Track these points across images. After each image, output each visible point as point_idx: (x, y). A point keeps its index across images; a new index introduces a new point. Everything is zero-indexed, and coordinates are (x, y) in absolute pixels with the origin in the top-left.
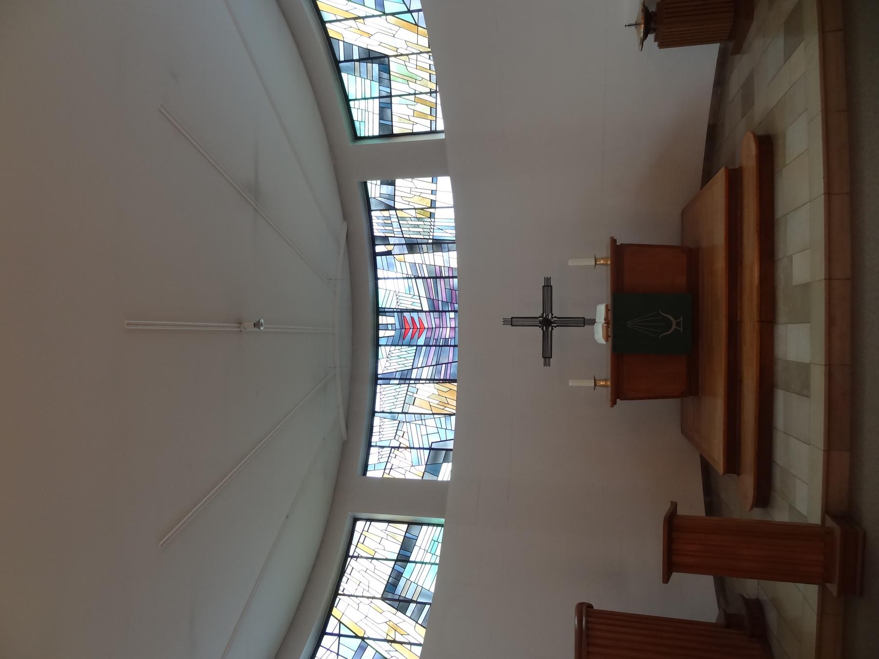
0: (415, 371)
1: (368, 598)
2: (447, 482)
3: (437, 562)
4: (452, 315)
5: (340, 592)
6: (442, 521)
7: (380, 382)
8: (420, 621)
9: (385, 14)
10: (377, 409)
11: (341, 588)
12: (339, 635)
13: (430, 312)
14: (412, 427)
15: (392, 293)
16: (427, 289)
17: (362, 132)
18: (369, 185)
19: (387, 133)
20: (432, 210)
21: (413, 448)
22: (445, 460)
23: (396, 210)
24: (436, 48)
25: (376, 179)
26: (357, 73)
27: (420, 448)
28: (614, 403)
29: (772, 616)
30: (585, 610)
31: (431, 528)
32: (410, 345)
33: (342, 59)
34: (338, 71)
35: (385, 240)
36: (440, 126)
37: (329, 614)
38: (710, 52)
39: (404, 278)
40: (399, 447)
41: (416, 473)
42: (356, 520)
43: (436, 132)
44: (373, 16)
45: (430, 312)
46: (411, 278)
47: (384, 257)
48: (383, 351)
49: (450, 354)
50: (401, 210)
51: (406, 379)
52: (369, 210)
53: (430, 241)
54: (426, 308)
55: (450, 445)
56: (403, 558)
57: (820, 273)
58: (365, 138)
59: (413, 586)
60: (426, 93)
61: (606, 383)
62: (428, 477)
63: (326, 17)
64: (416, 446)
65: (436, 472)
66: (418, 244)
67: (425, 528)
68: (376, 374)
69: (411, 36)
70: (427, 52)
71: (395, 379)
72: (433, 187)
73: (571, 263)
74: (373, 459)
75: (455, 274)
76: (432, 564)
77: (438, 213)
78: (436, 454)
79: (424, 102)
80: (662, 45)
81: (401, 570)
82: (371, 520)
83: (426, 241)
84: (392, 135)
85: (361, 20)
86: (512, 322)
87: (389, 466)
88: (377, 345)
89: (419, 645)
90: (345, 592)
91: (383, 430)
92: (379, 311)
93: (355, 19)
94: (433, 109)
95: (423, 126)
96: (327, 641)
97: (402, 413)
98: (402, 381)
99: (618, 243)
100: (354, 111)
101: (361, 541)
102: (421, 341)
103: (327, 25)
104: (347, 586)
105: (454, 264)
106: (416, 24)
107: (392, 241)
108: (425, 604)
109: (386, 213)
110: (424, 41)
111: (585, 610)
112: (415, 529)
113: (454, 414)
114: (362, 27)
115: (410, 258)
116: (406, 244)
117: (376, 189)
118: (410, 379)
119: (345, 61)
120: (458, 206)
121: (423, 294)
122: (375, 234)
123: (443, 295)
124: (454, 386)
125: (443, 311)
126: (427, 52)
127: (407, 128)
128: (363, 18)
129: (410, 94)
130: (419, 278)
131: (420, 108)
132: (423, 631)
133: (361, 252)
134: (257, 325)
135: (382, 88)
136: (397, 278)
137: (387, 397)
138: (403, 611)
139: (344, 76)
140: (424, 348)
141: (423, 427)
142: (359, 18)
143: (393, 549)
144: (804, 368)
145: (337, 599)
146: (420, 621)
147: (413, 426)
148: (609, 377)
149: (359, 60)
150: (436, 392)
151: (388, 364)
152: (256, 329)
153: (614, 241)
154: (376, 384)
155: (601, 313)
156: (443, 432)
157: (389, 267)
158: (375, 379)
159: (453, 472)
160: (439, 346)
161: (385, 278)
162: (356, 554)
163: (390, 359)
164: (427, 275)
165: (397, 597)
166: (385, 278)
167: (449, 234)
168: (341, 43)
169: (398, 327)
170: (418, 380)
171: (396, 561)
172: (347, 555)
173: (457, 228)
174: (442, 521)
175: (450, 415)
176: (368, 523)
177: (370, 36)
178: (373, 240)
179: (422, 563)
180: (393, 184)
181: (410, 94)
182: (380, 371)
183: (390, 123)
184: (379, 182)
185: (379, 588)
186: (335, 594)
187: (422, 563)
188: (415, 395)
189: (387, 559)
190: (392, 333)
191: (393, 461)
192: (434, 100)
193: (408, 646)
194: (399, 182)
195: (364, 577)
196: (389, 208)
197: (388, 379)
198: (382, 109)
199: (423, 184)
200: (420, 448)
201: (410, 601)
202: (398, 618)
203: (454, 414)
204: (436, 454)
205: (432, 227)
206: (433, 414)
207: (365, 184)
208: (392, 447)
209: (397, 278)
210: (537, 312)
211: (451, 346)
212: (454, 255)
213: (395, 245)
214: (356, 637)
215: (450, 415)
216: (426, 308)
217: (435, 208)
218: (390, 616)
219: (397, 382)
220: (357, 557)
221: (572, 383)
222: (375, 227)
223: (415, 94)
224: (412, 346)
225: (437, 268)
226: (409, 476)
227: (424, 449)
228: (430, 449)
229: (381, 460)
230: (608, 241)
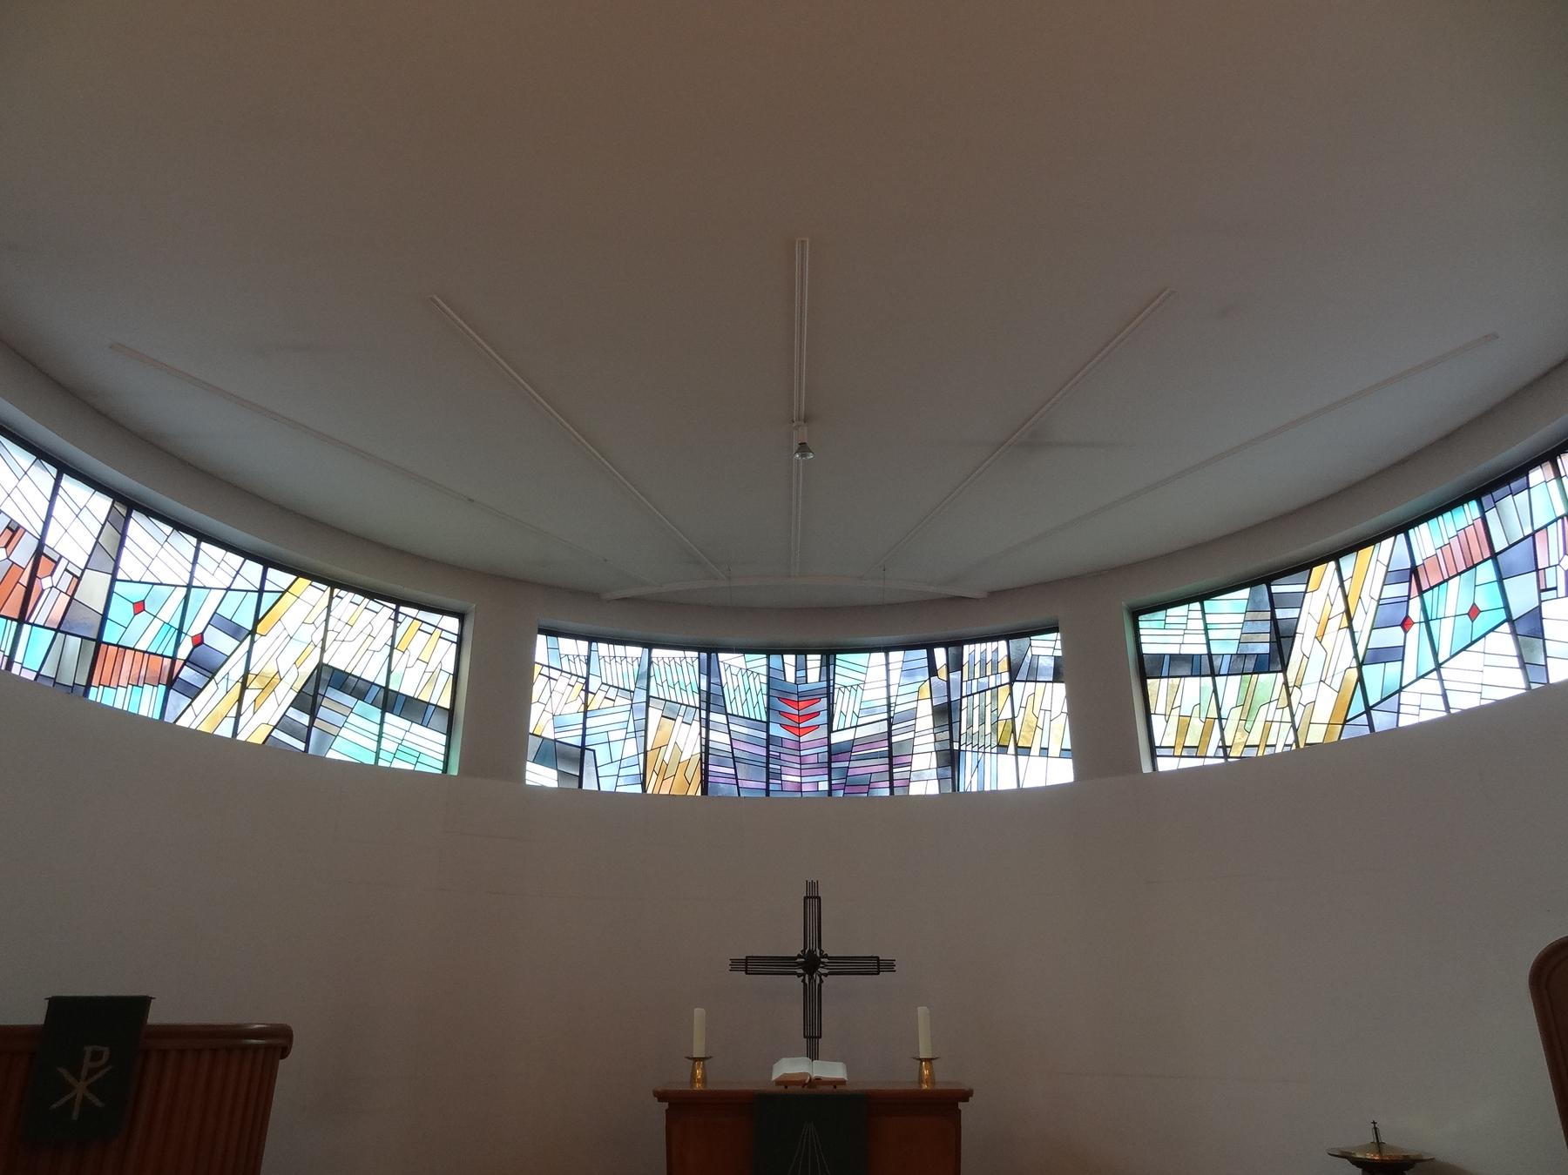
0: (722, 718)
1: (324, 640)
2: (523, 779)
3: (381, 763)
4: (824, 786)
5: (336, 591)
7: (704, 655)
8: (278, 734)
9: (1360, 666)
11: (343, 593)
12: (261, 591)
13: (829, 745)
14: (621, 714)
15: (862, 677)
16: (869, 741)
17: (1147, 624)
18: (1053, 636)
19: (1148, 667)
20: (1011, 749)
21: (585, 718)
22: (562, 775)
23: (1011, 684)
24: (1304, 757)
25: (1063, 649)
26: (1250, 616)
27: (584, 729)
28: (661, 1096)
30: (278, 1041)
31: (443, 750)
32: (768, 709)
33: (1274, 589)
35: (956, 664)
36: (1165, 765)
37: (299, 572)
39: (889, 698)
40: (587, 691)
41: (541, 722)
42: (461, 616)
43: (1153, 756)
44: (1355, 645)
45: (829, 745)
46: (889, 711)
47: (925, 662)
48: (758, 662)
49: (753, 783)
50: (1011, 694)
51: (708, 704)
52: (1008, 636)
53: (956, 746)
55: (589, 784)
56: (390, 702)
58: (1136, 629)
59: (339, 719)
60: (1222, 739)
61: (699, 1080)
62: (533, 744)
63: (1347, 563)
64: (589, 723)
65: (540, 759)
67: (443, 739)
69: (1323, 713)
70: (1296, 741)
72: (1054, 750)
73: (922, 1011)
74: (567, 645)
75: (897, 792)
76: (377, 753)
77: (1007, 760)
78: (572, 757)
79: (1206, 734)
82: (459, 644)
83: (956, 737)
84: (1143, 677)
85: (1345, 623)
86: (812, 899)
88: (768, 651)
89: (235, 733)
90: (336, 601)
91: (619, 662)
92: (829, 654)
93: (1347, 611)
94: (1196, 751)
95: (1164, 732)
96: (253, 570)
97: (648, 697)
98: (704, 696)
99: (961, 1105)
100: (1181, 610)
101: (424, 627)
102: (776, 730)
103: (1332, 564)
104: (347, 602)
105: (916, 789)
106: (1346, 721)
107: (955, 676)
108: (307, 742)
109: (1003, 666)
110: (1316, 735)
111: (278, 1041)
112: (442, 722)
113: (644, 789)
114: (1333, 625)
115: (925, 709)
116: (950, 702)
117: (1046, 648)
118: (708, 711)
119: (1271, 595)
120: (1022, 799)
121: (862, 732)
122: (967, 649)
123: (859, 769)
124: (695, 790)
125: (830, 769)
126: (1296, 741)
127: (1159, 703)
128: (1350, 627)
129: (1219, 709)
130: (890, 725)
131: (1197, 726)
132: (258, 739)
133: (933, 622)
134: (803, 448)
135: (1227, 659)
136: (888, 686)
137: (677, 669)
138: (295, 704)
139: (1245, 593)
140: (764, 735)
141: (622, 734)
142: (1350, 619)
143: (407, 684)
145: (324, 587)
146: (278, 734)
147: (625, 716)
148: (710, 1087)
149: (1273, 619)
150: (685, 757)
151: (735, 671)
152: (795, 446)
153: (966, 1096)
154: (700, 650)
155: (831, 1070)
156: (611, 773)
157: (908, 672)
158: (710, 649)
159: (541, 790)
160: (768, 763)
161: (887, 664)
162: (401, 617)
163: (743, 673)
164: (894, 739)
165: (321, 691)
166: (887, 664)
167: (969, 781)
168: (1302, 588)
169: (802, 688)
171: (386, 689)
172: (400, 601)
173: (981, 794)
174: (454, 770)
175: (643, 784)
176: (455, 639)
177: (1319, 638)
178: (955, 644)
179: (380, 736)
180: (1057, 677)
181: (1219, 709)
182: (722, 656)
183: (1165, 673)
184: (1059, 653)
185: (339, 659)
186: (334, 583)
187: (380, 736)
188: (679, 719)
189: (389, 672)
190: (790, 678)
191: (563, 681)
192: (1211, 752)
193: (233, 713)
194: (1061, 689)
195: (361, 633)
196: (1013, 672)
197: (709, 670)
198: (1190, 659)
199: (1059, 734)
200: (584, 729)
201: (313, 716)
202: (285, 693)
203: (644, 789)
204: (572, 757)
205: (981, 750)
206: (645, 753)
207: (1054, 629)
208: (587, 679)
209: (888, 686)
210: (831, 947)
211: (768, 784)
212: (933, 788)
213: (948, 681)
214: (257, 621)
215: (643, 784)
216: (836, 738)
217: (1016, 755)
218: (289, 679)
219: (704, 686)
220: (396, 620)
221: (699, 1012)
222: (979, 648)
223: (1220, 718)
225: (908, 759)
226: (535, 710)
227: (584, 736)
228: (583, 748)
229: (565, 660)
230: (966, 1086)
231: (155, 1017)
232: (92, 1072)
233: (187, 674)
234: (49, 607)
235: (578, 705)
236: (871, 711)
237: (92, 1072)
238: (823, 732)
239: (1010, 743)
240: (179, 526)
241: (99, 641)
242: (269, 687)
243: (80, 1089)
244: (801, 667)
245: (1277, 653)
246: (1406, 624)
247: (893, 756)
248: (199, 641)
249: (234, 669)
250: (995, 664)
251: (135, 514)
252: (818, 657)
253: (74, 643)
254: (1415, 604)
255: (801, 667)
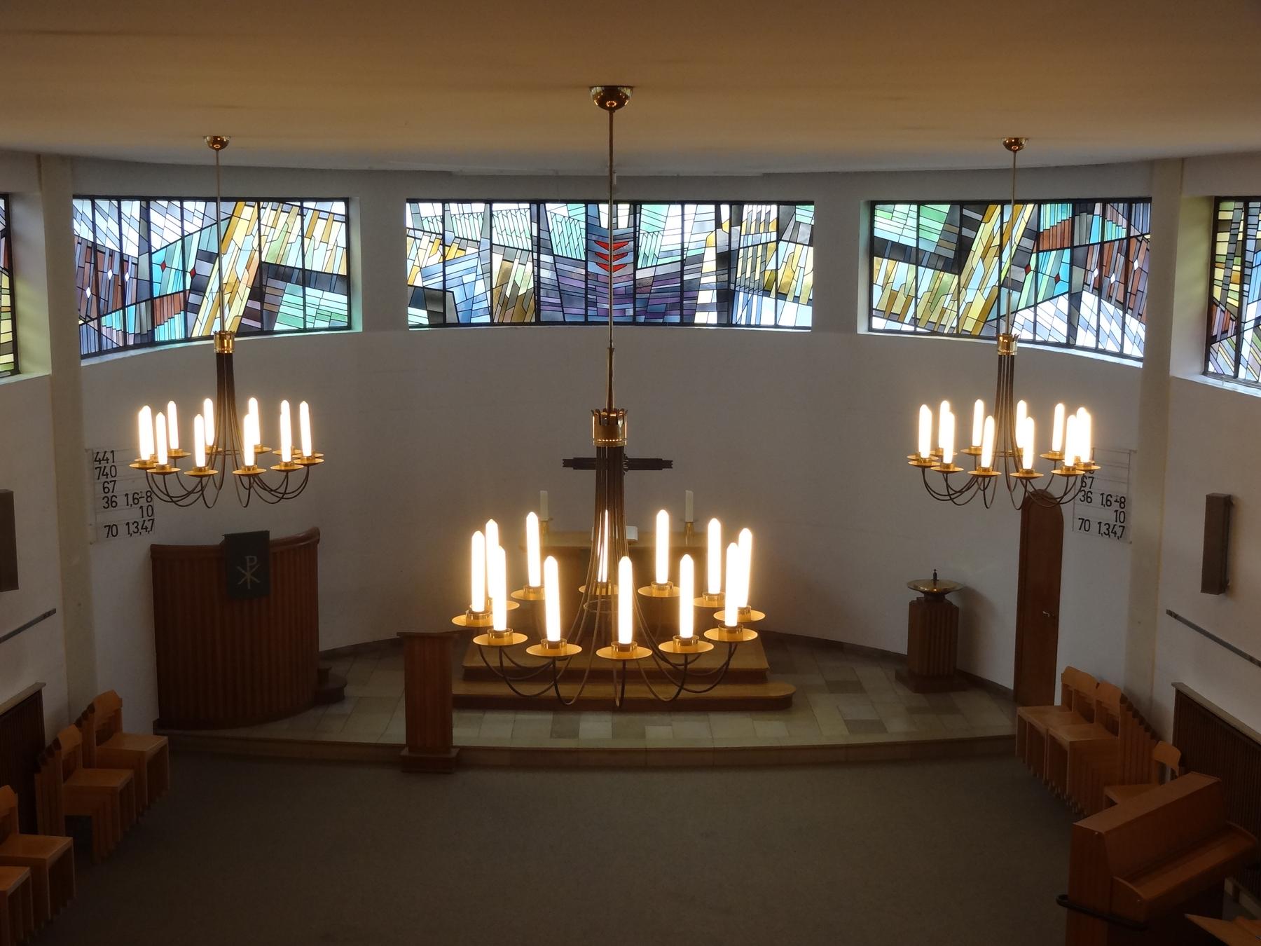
1: (260, 245)
4: (631, 312)
6: (358, 327)
10: (496, 206)
13: (635, 280)
15: (662, 225)
16: (667, 278)
18: (812, 208)
19: (878, 248)
21: (444, 267)
27: (444, 275)
29: (334, 709)
31: (346, 307)
32: (587, 250)
33: (966, 212)
34: (952, 203)
35: (737, 220)
36: (878, 323)
37: (237, 200)
38: (902, 648)
39: (683, 243)
40: (444, 245)
42: (347, 201)
46: (682, 255)
47: (713, 216)
48: (578, 210)
50: (777, 250)
51: (539, 246)
52: (779, 203)
53: (732, 286)
54: (640, 275)
56: (307, 278)
57: (650, 745)
58: (872, 216)
63: (1008, 208)
64: (448, 270)
66: (729, 270)
68: (545, 201)
69: (975, 312)
71: (539, 229)
72: (804, 300)
76: (304, 318)
77: (769, 302)
78: (434, 299)
80: (912, 604)
81: (294, 280)
83: (733, 279)
87: (419, 234)
91: (466, 218)
92: (636, 206)
97: (492, 244)
101: (322, 215)
102: (593, 267)
105: (700, 318)
107: (736, 229)
109: (773, 227)
115: (710, 255)
117: (805, 215)
118: (539, 253)
122: (746, 207)
130: (683, 266)
131: (901, 299)
136: (683, 233)
137: (513, 221)
140: (583, 272)
143: (316, 263)
144: (575, 734)
145: (252, 203)
150: (522, 292)
154: (531, 202)
160: (586, 294)
161: (683, 214)
163: (566, 222)
166: (683, 214)
167: (740, 315)
169: (615, 232)
170: (538, 264)
171: (303, 270)
174: (358, 327)
176: (343, 219)
178: (737, 205)
179: (304, 306)
182: (549, 206)
186: (258, 200)
188: (516, 261)
189: (303, 256)
190: (605, 224)
191: (426, 239)
194: (811, 249)
197: (538, 218)
200: (444, 275)
201: (262, 303)
206: (492, 289)
208: (443, 235)
209: (683, 233)
211: (586, 310)
213: (730, 234)
215: (491, 314)
216: (640, 275)
217: (776, 298)
218: (244, 282)
219: (535, 233)
223: (916, 297)
224: (586, 254)
228: (444, 290)
229: (425, 222)
231: (272, 537)
232: (251, 567)
233: (193, 298)
234: (131, 296)
235: (437, 257)
236: (670, 253)
237: (251, 567)
238: (630, 269)
239: (772, 289)
240: (169, 199)
241: (152, 299)
242: (234, 292)
243: (248, 575)
244: (613, 215)
245: (955, 258)
246: (1027, 269)
247: (684, 292)
248: (193, 273)
249: (213, 285)
250: (767, 223)
251: (152, 203)
252: (627, 206)
253: (143, 305)
254: (1034, 256)
255: (613, 215)
